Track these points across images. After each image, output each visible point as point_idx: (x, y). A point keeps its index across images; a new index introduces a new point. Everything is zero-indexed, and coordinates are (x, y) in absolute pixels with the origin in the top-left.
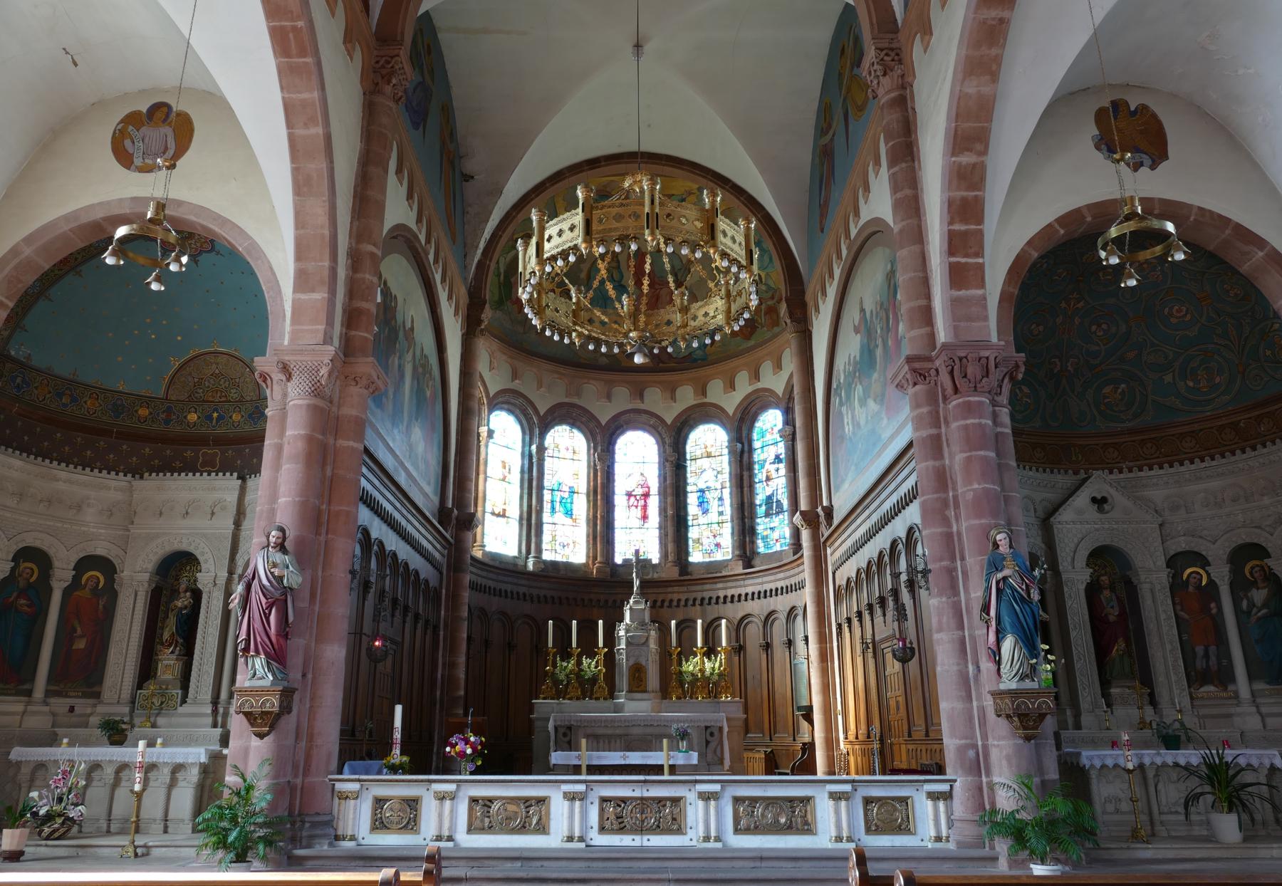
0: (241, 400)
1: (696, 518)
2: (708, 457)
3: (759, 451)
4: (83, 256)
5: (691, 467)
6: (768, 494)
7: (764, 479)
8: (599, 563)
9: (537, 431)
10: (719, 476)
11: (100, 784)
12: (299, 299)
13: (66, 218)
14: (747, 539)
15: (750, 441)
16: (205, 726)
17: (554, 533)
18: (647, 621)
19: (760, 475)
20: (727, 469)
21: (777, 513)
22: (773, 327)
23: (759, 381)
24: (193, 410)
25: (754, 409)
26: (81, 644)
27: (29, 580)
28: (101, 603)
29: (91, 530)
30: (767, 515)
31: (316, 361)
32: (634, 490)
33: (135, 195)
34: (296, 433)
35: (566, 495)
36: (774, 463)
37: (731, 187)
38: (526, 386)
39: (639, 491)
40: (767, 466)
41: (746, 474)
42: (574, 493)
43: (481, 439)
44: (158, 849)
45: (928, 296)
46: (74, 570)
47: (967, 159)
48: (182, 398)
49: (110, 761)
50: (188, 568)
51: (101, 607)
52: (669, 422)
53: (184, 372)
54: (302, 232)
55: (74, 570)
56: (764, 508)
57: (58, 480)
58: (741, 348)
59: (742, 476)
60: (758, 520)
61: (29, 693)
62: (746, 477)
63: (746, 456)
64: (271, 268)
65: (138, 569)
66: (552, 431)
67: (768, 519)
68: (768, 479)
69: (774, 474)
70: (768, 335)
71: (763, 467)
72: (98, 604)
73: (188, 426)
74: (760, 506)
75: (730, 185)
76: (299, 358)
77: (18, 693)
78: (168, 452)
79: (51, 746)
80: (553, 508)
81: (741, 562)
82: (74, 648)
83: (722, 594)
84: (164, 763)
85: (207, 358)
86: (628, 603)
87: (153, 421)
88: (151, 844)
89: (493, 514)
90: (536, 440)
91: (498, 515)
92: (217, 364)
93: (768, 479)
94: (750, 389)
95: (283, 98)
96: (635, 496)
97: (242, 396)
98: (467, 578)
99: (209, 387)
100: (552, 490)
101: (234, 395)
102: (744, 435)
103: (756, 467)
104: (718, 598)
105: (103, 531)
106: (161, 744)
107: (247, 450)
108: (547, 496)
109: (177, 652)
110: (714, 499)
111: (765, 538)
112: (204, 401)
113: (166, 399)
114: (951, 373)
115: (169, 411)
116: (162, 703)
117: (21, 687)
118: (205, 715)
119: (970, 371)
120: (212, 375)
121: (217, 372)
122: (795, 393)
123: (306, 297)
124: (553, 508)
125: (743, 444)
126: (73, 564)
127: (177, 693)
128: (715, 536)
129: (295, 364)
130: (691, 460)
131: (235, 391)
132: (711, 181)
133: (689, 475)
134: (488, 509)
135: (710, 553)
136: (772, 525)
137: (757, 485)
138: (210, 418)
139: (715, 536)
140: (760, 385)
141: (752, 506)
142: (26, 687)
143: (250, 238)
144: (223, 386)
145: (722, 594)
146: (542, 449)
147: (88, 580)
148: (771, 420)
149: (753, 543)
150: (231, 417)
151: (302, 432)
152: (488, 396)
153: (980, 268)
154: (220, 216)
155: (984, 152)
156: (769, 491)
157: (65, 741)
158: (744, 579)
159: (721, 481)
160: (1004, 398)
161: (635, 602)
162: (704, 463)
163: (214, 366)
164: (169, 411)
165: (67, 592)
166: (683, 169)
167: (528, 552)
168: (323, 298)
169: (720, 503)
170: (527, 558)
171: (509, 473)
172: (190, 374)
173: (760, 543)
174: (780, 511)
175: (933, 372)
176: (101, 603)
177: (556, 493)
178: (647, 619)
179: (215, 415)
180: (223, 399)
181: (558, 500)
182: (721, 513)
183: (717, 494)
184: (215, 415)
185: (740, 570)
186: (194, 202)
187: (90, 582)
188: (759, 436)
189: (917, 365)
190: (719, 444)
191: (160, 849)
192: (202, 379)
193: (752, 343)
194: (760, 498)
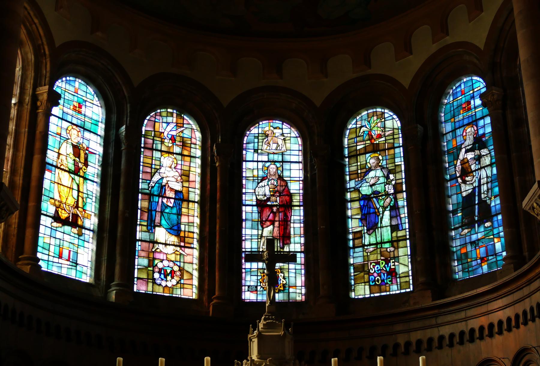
1: (358, 235)
2: (374, 151)
3: (449, 137)
8: (217, 298)
10: (392, 177)
15: (436, 123)
17: (151, 256)
18: (288, 357)
21: (481, 222)
23: (447, 34)
32: (268, 199)
35: (171, 203)
39: (276, 201)
42: (183, 200)
43: (39, 103)
52: (318, 103)
74: (455, 212)
81: (429, 293)
83: (401, 340)
86: (255, 327)
89: (56, 218)
90: (127, 119)
91: (65, 222)
94: (434, 48)
96: (271, 206)
104: (397, 346)
108: (142, 204)
110: (384, 208)
111: (464, 258)
122: (516, 12)
128: (387, 261)
134: (47, 207)
135: (381, 286)
139: (387, 261)
140: (449, 40)
145: (401, 340)
152: (51, 42)
156: (466, 189)
158: (436, 316)
161: (267, 326)
162: (370, 160)
167: (110, 277)
169: (394, 214)
170: (108, 287)
177: (156, 199)
178: (289, 354)
181: (159, 209)
182: (394, 228)
185: (429, 302)
188: (449, 116)
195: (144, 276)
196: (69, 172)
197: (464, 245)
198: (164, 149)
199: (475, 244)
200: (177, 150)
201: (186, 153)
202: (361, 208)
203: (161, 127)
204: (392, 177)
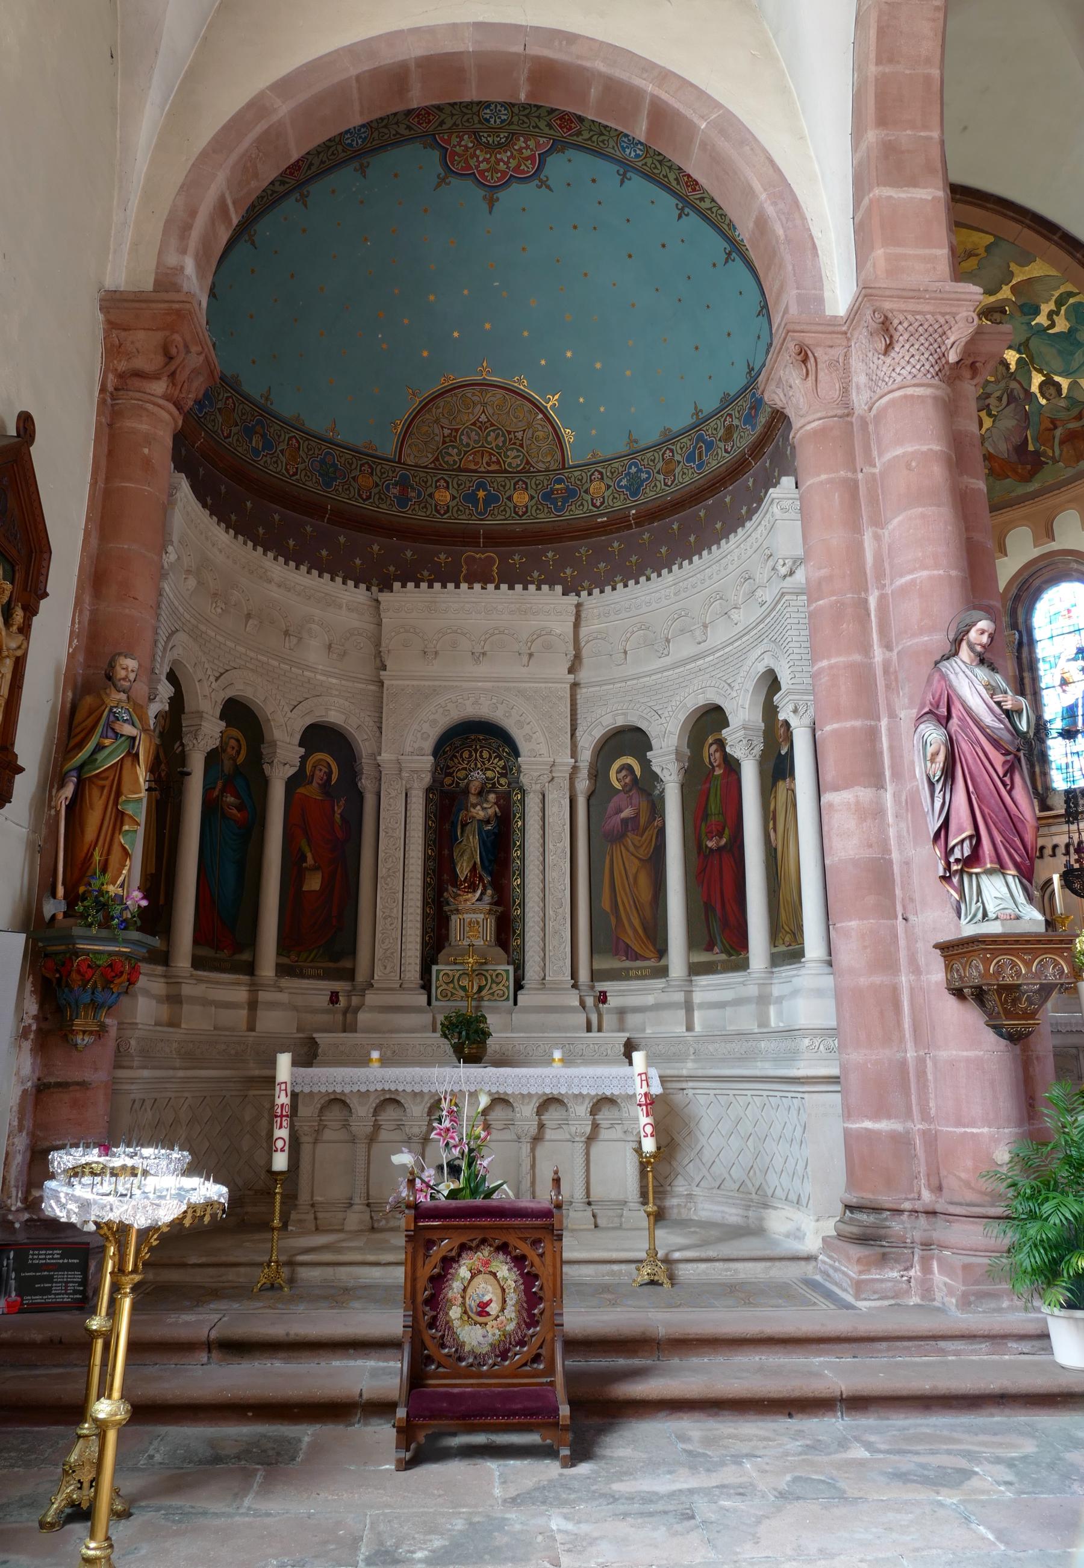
0: (527, 469)
4: (322, 162)
7: (1058, 682)
11: (508, 1135)
12: (891, 197)
13: (351, 51)
14: (1037, 769)
15: (1030, 631)
16: (575, 1029)
22: (1078, 461)
23: (1054, 540)
24: (442, 483)
25: (1037, 583)
26: (314, 883)
27: (235, 761)
28: (338, 811)
29: (319, 677)
31: (943, 314)
33: (480, 19)
34: (925, 448)
37: (1060, 238)
40: (1062, 663)
41: (1027, 675)
44: (689, 1266)
46: (300, 745)
48: (424, 461)
49: (415, 1094)
50: (466, 755)
51: (337, 816)
53: (427, 416)
54: (888, 69)
55: (300, 745)
57: (270, 581)
58: (1013, 494)
59: (1022, 679)
60: (1050, 742)
61: (250, 969)
62: (1027, 681)
63: (1025, 650)
64: (772, 162)
65: (408, 749)
68: (1064, 682)
70: (1070, 472)
72: (334, 812)
73: (437, 511)
75: (1059, 235)
76: (911, 306)
77: (235, 969)
78: (409, 553)
79: (311, 1066)
82: (305, 888)
84: (576, 1096)
85: (468, 392)
87: (380, 498)
88: (677, 1255)
92: (484, 404)
93: (1064, 682)
94: (1036, 552)
97: (528, 463)
99: (468, 445)
101: (513, 459)
102: (1021, 620)
105: (334, 681)
106: (562, 1060)
107: (675, 526)
109: (487, 898)
112: (459, 469)
113: (399, 462)
115: (404, 484)
116: (481, 989)
117: (237, 957)
118: (570, 1009)
120: (474, 424)
121: (483, 418)
123: (903, 195)
126: (298, 737)
127: (507, 971)
129: (902, 318)
131: (515, 453)
132: (1029, 227)
138: (472, 498)
140: (1054, 546)
142: (246, 956)
143: (718, 105)
144: (493, 445)
147: (314, 767)
149: (1045, 774)
150: (510, 498)
151: (936, 447)
154: (653, 66)
156: (1068, 700)
157: (557, 1055)
163: (478, 409)
164: (404, 484)
165: (292, 784)
166: (987, 209)
168: (934, 198)
172: (437, 421)
176: (338, 811)
179: (481, 494)
180: (494, 467)
184: (481, 494)
186: (600, 38)
187: (317, 772)
191: (695, 1265)
192: (457, 430)
193: (1034, 486)
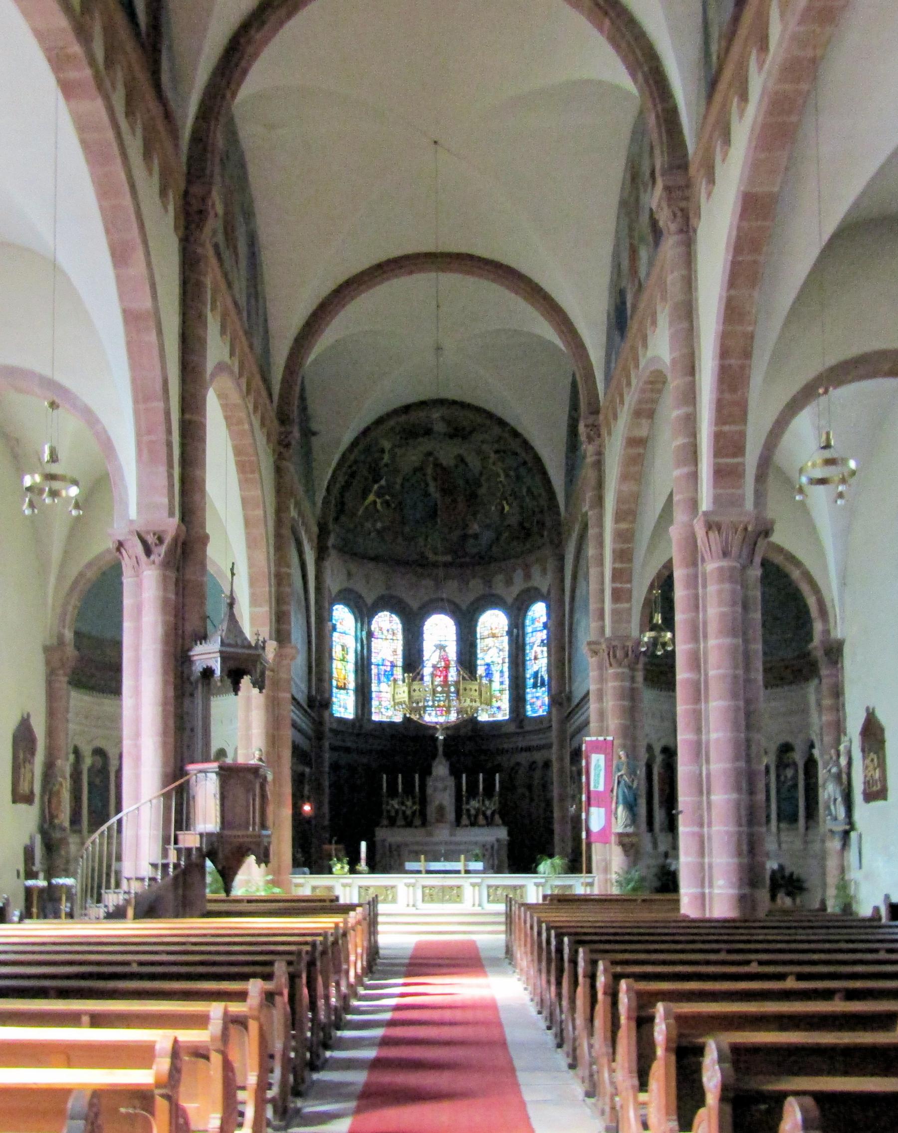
2: (493, 637)
3: (530, 635)
5: (480, 645)
6: (535, 670)
7: (533, 658)
9: (366, 620)
19: (530, 655)
20: (507, 648)
30: (535, 686)
35: (388, 669)
36: (540, 646)
38: (359, 586)
40: (536, 648)
45: (603, 601)
47: (623, 526)
56: (532, 681)
60: (528, 690)
66: (377, 617)
67: (534, 690)
68: (536, 658)
69: (540, 656)
71: (532, 649)
74: (530, 679)
80: (379, 679)
90: (366, 627)
93: (536, 658)
95: (241, 495)
98: (326, 744)
100: (378, 665)
103: (528, 647)
111: (532, 704)
114: (609, 654)
119: (618, 655)
124: (379, 679)
125: (518, 630)
130: (481, 639)
133: (479, 651)
136: (537, 695)
137: (528, 663)
141: (524, 679)
146: (370, 635)
148: (538, 611)
149: (524, 707)
153: (630, 591)
155: (633, 521)
159: (502, 657)
160: (640, 666)
162: (490, 641)
171: (347, 654)
173: (528, 707)
174: (543, 685)
175: (601, 651)
182: (502, 683)
183: (499, 668)
189: (593, 647)
190: (501, 626)
194: (529, 674)
195: (377, 711)
196: (341, 660)
197: (533, 698)
198: (384, 637)
199: (537, 698)
200: (390, 637)
201: (394, 638)
202: (486, 670)
203: (382, 625)
204: (501, 653)
